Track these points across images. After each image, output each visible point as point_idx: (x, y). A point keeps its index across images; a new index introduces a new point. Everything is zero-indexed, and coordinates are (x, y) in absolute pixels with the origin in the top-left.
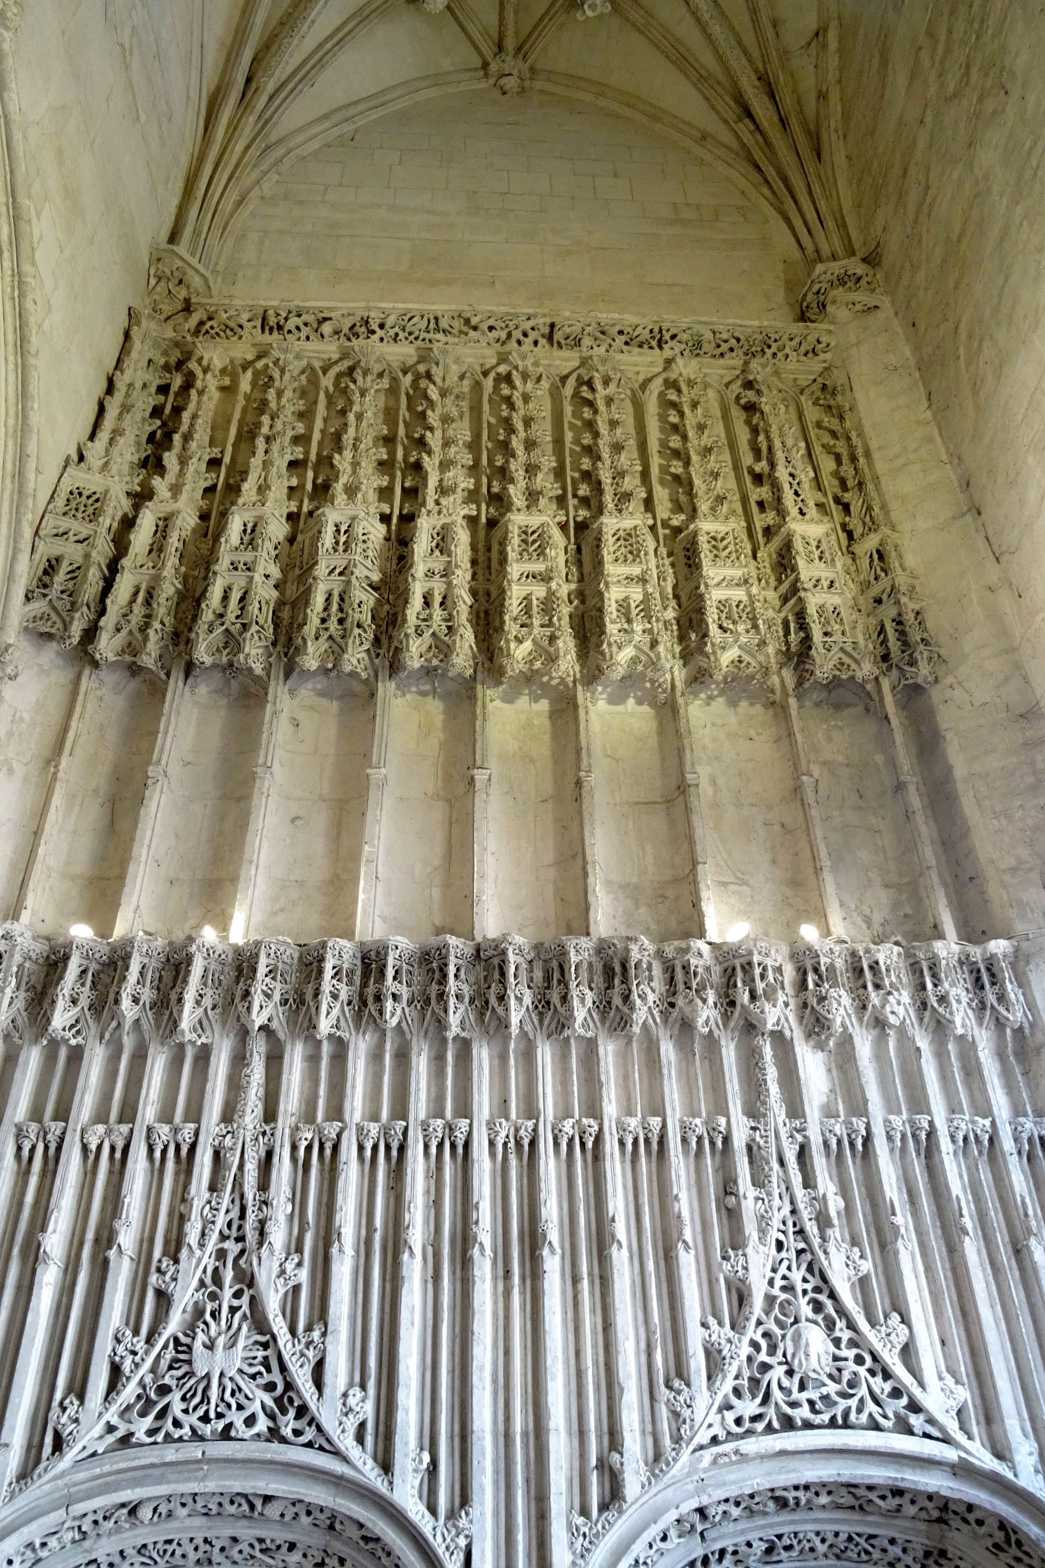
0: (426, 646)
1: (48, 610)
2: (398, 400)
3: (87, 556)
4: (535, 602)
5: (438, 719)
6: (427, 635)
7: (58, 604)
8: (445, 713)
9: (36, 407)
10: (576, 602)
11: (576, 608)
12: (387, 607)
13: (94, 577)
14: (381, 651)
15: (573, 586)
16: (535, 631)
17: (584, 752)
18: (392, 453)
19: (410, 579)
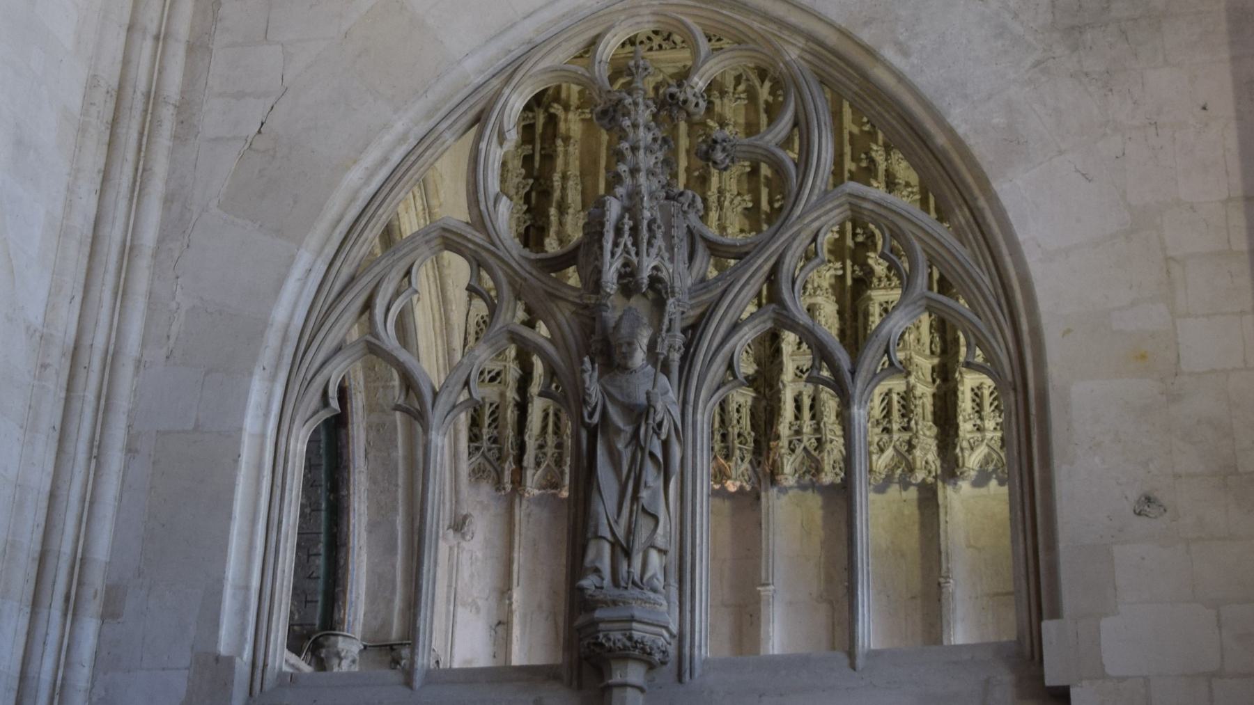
0: (799, 460)
1: (481, 460)
2: (757, 111)
3: (502, 395)
4: (895, 398)
5: (818, 514)
6: (799, 450)
7: (489, 455)
8: (825, 507)
9: (454, 308)
10: (938, 381)
11: (938, 388)
12: (764, 403)
13: (511, 415)
14: (761, 459)
15: (936, 361)
16: (896, 436)
17: (943, 555)
18: (757, 201)
19: (781, 385)
